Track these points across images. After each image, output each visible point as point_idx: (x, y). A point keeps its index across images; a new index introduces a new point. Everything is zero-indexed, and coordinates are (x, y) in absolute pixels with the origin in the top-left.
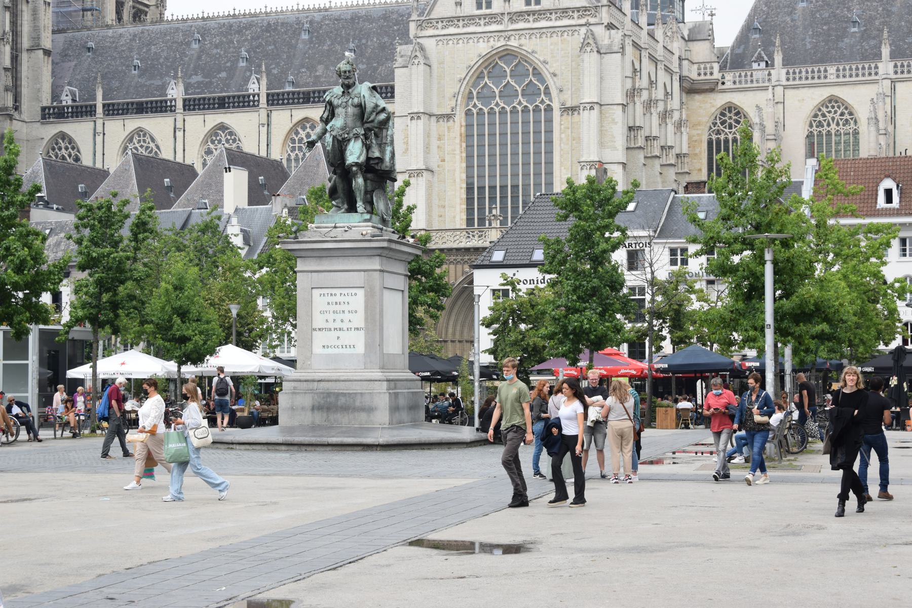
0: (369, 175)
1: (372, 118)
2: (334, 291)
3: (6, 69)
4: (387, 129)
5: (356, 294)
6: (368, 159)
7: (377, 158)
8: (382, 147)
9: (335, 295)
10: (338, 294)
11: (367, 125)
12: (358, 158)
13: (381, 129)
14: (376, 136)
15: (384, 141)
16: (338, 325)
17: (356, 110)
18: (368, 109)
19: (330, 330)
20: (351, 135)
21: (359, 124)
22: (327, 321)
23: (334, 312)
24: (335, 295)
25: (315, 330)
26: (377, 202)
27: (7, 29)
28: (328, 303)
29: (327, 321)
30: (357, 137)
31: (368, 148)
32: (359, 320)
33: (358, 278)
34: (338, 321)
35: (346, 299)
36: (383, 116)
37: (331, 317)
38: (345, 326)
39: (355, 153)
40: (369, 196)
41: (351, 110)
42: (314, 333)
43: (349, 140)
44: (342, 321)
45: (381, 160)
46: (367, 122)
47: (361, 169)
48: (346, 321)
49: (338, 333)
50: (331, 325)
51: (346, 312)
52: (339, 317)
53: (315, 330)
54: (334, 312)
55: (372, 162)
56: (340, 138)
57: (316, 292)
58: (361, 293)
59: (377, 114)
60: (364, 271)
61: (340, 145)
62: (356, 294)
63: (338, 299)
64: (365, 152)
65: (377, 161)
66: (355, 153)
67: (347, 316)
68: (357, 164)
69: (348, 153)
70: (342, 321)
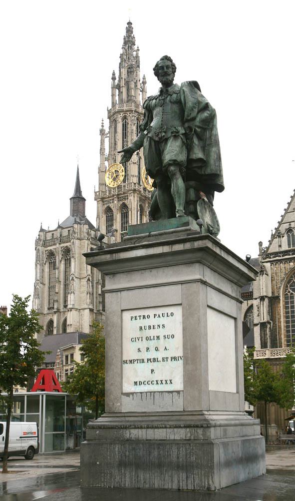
0: (192, 183)
1: (193, 114)
2: (146, 313)
3: (99, 295)
4: (212, 130)
5: (172, 314)
6: (190, 161)
7: (200, 160)
8: (205, 148)
9: (149, 317)
10: (152, 316)
11: (186, 125)
12: (177, 155)
13: (204, 130)
14: (200, 138)
15: (208, 143)
16: (152, 354)
17: (176, 107)
18: (189, 104)
19: (143, 361)
20: (169, 134)
21: (177, 123)
22: (139, 350)
23: (148, 339)
24: (149, 317)
25: (126, 362)
26: (201, 211)
27: (100, 278)
28: (141, 328)
29: (139, 350)
30: (176, 137)
31: (189, 147)
32: (176, 347)
33: (174, 294)
34: (152, 349)
35: (162, 321)
36: (206, 114)
37: (143, 345)
38: (159, 355)
39: (173, 151)
40: (192, 207)
41: (169, 107)
42: (125, 366)
43: (166, 140)
44: (157, 349)
45: (203, 162)
46: (188, 121)
47: (181, 171)
48: (161, 349)
49: (151, 365)
50: (146, 356)
51: (162, 338)
52: (152, 344)
53: (126, 362)
54: (148, 339)
55: (195, 165)
56: (157, 139)
57: (127, 316)
58: (178, 312)
59: (199, 112)
60: (182, 283)
61: (157, 146)
62: (172, 314)
63: (152, 321)
64: (185, 152)
65: (200, 165)
66: (173, 151)
67: (162, 343)
68: (175, 163)
69: (166, 152)
70: (157, 349)
